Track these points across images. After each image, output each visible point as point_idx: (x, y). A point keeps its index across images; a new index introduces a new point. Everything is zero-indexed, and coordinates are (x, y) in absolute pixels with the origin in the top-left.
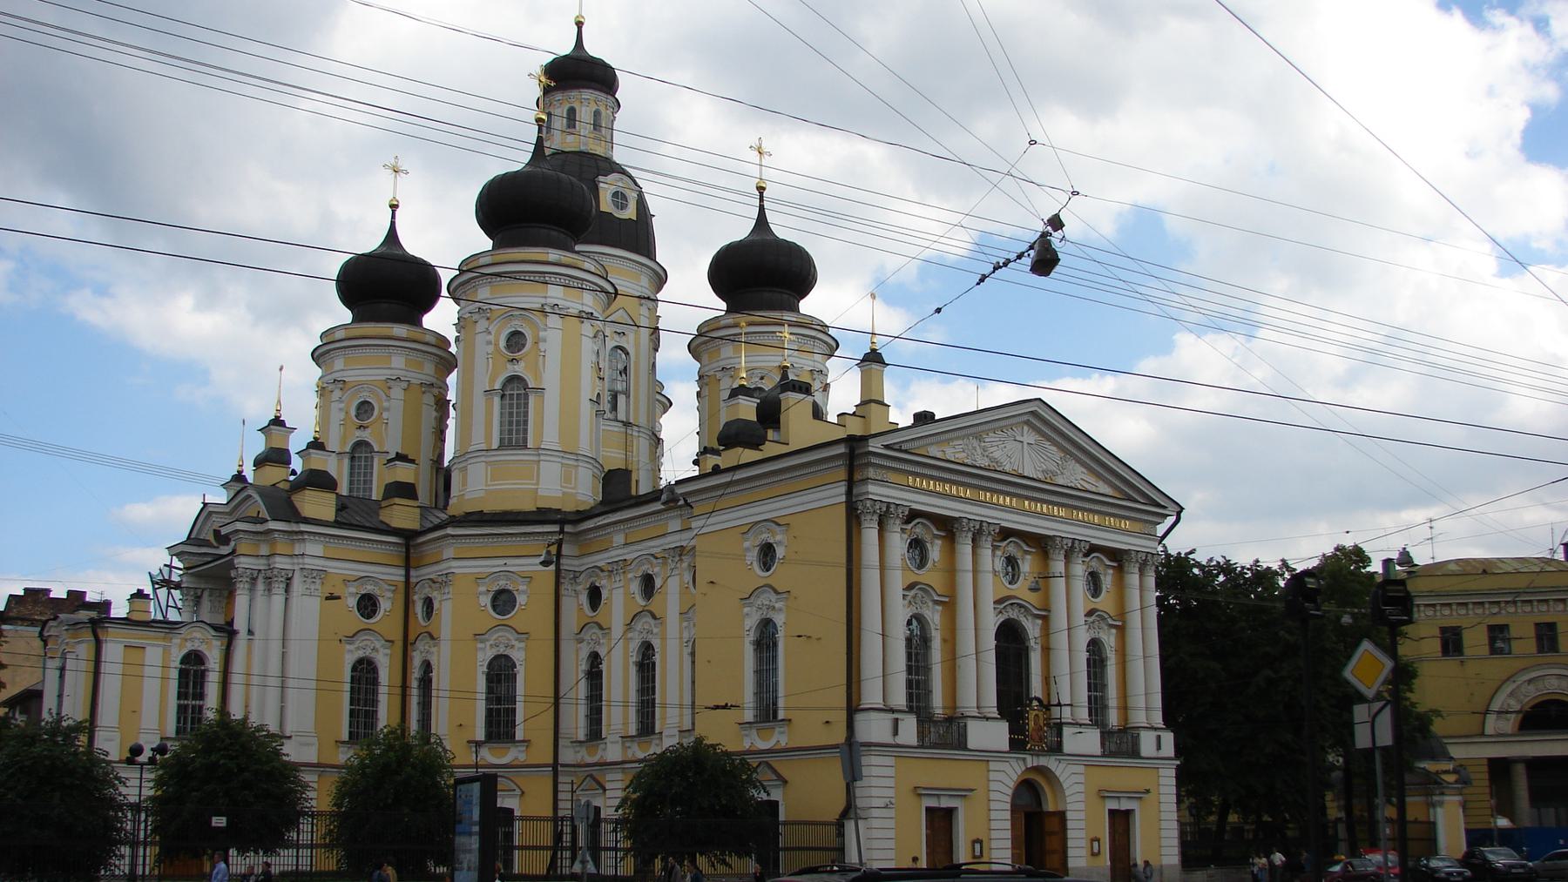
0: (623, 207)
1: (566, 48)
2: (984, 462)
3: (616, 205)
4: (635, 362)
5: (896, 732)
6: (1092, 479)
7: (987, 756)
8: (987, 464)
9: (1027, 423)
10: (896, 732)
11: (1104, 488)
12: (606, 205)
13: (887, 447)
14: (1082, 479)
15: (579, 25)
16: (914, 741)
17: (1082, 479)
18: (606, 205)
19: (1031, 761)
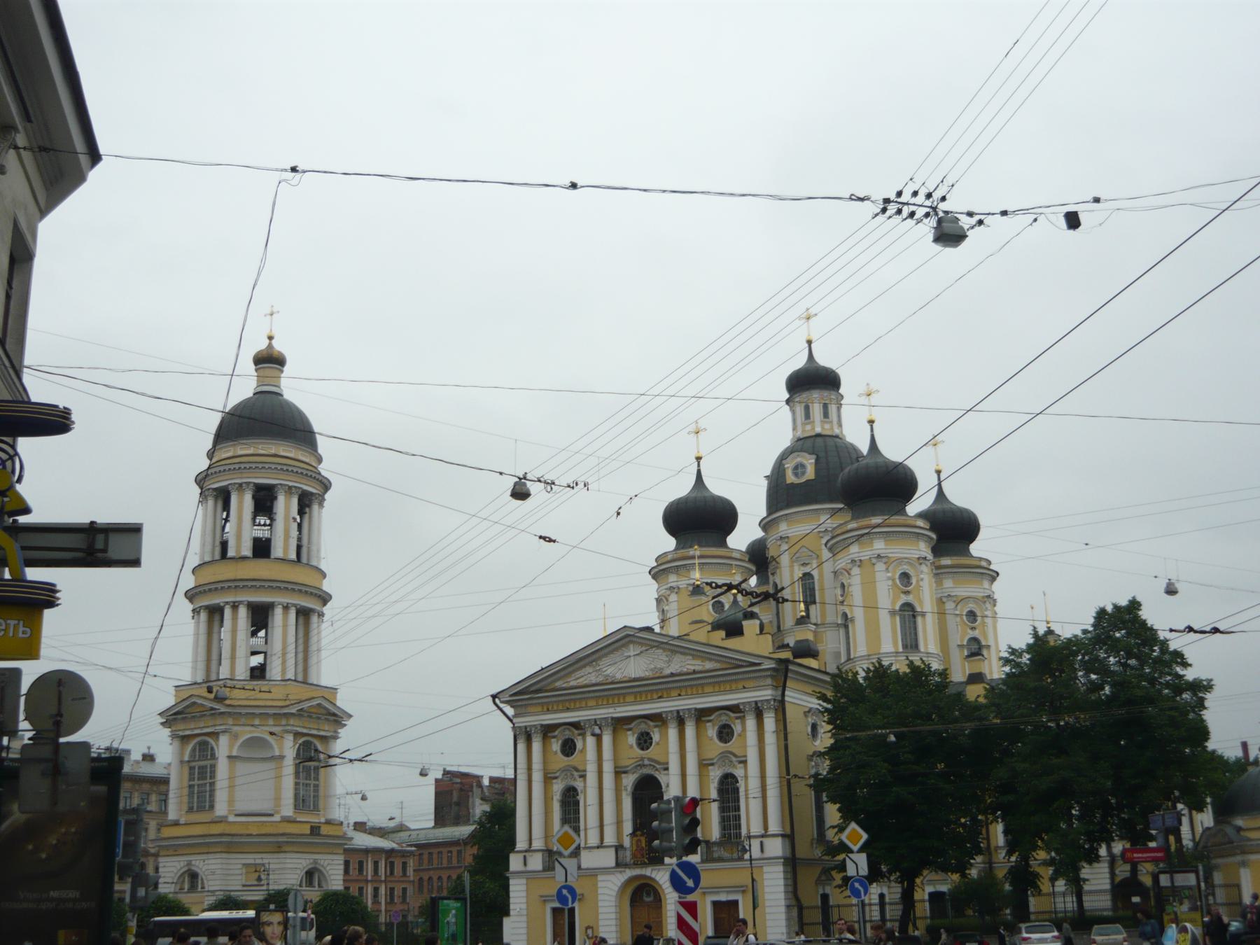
0: (803, 473)
1: (800, 362)
2: (600, 679)
3: (796, 475)
4: (819, 580)
5: (525, 864)
6: (699, 662)
7: (593, 873)
8: (601, 679)
9: (631, 642)
10: (525, 864)
11: (709, 665)
12: (791, 478)
13: (511, 696)
14: (688, 664)
15: (809, 342)
16: (540, 867)
17: (688, 664)
18: (791, 478)
19: (629, 873)
